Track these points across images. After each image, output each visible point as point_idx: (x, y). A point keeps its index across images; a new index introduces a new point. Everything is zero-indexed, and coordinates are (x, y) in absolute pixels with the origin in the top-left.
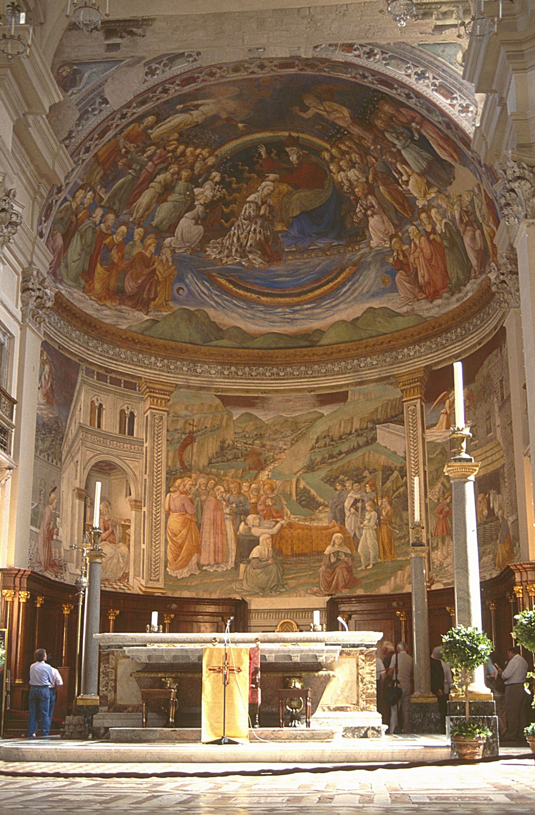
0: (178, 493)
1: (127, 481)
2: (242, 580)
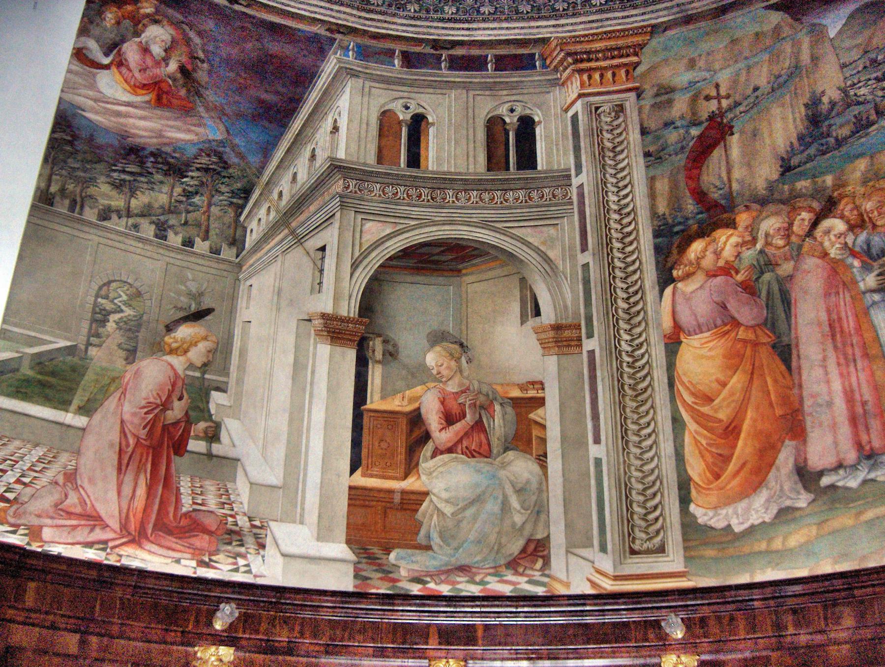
0: (698, 280)
1: (523, 281)
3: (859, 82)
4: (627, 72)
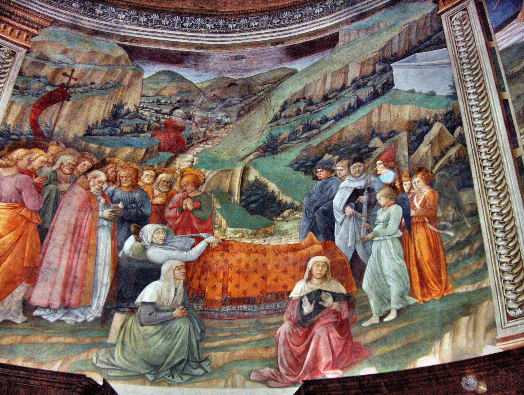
2: (114, 345)
3: (147, 108)
4: (28, 36)
